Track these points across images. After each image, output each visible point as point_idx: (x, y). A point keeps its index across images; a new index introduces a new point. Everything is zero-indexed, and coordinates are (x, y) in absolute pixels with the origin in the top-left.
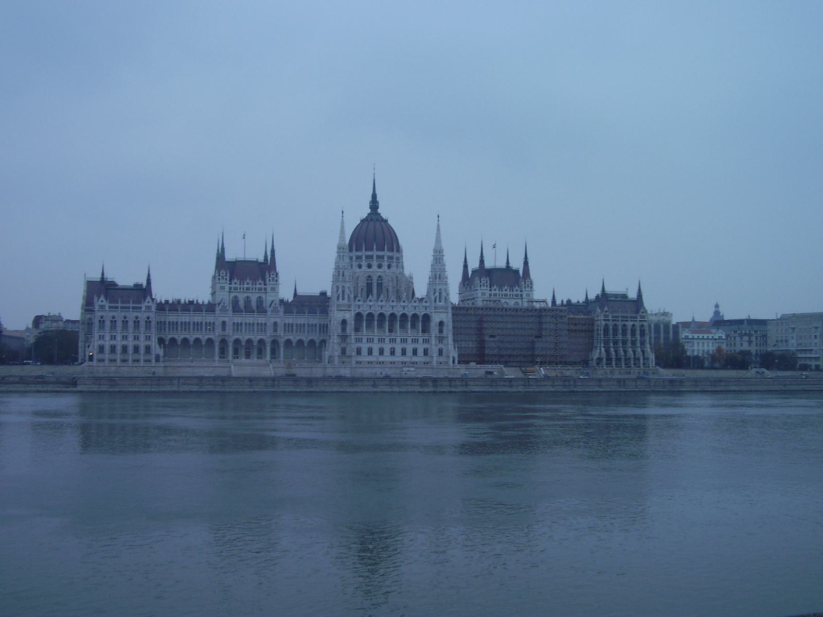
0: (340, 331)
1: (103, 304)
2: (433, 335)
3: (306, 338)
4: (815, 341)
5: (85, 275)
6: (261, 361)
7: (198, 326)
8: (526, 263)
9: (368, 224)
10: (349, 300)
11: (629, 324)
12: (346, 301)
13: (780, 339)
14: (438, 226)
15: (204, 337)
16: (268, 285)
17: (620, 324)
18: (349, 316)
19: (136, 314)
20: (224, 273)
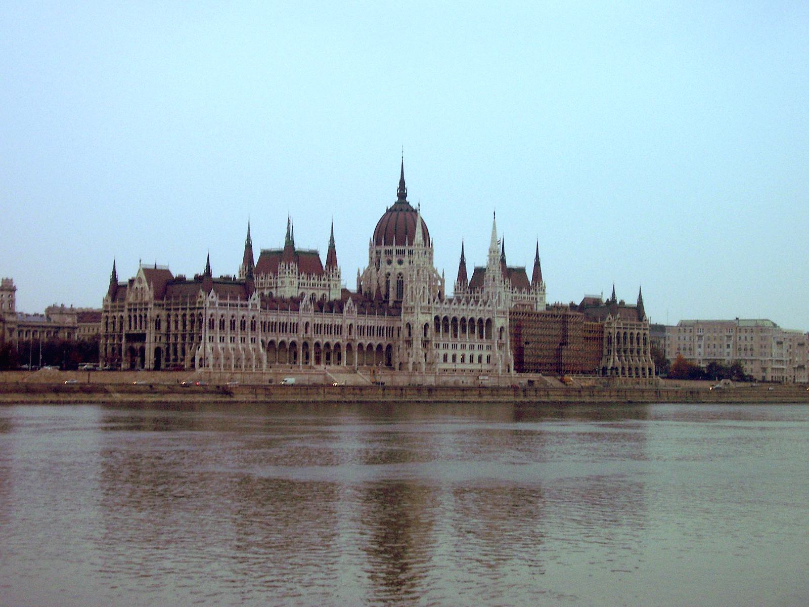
0: (422, 335)
1: (214, 299)
2: (496, 342)
3: (375, 341)
4: (728, 350)
5: (140, 261)
6: (339, 368)
7: (283, 327)
8: (537, 264)
9: (398, 215)
10: (429, 303)
11: (636, 332)
12: (425, 304)
13: (682, 347)
14: (494, 222)
15: (288, 338)
16: (332, 281)
17: (629, 332)
18: (430, 319)
19: (242, 313)
20: (294, 265)
